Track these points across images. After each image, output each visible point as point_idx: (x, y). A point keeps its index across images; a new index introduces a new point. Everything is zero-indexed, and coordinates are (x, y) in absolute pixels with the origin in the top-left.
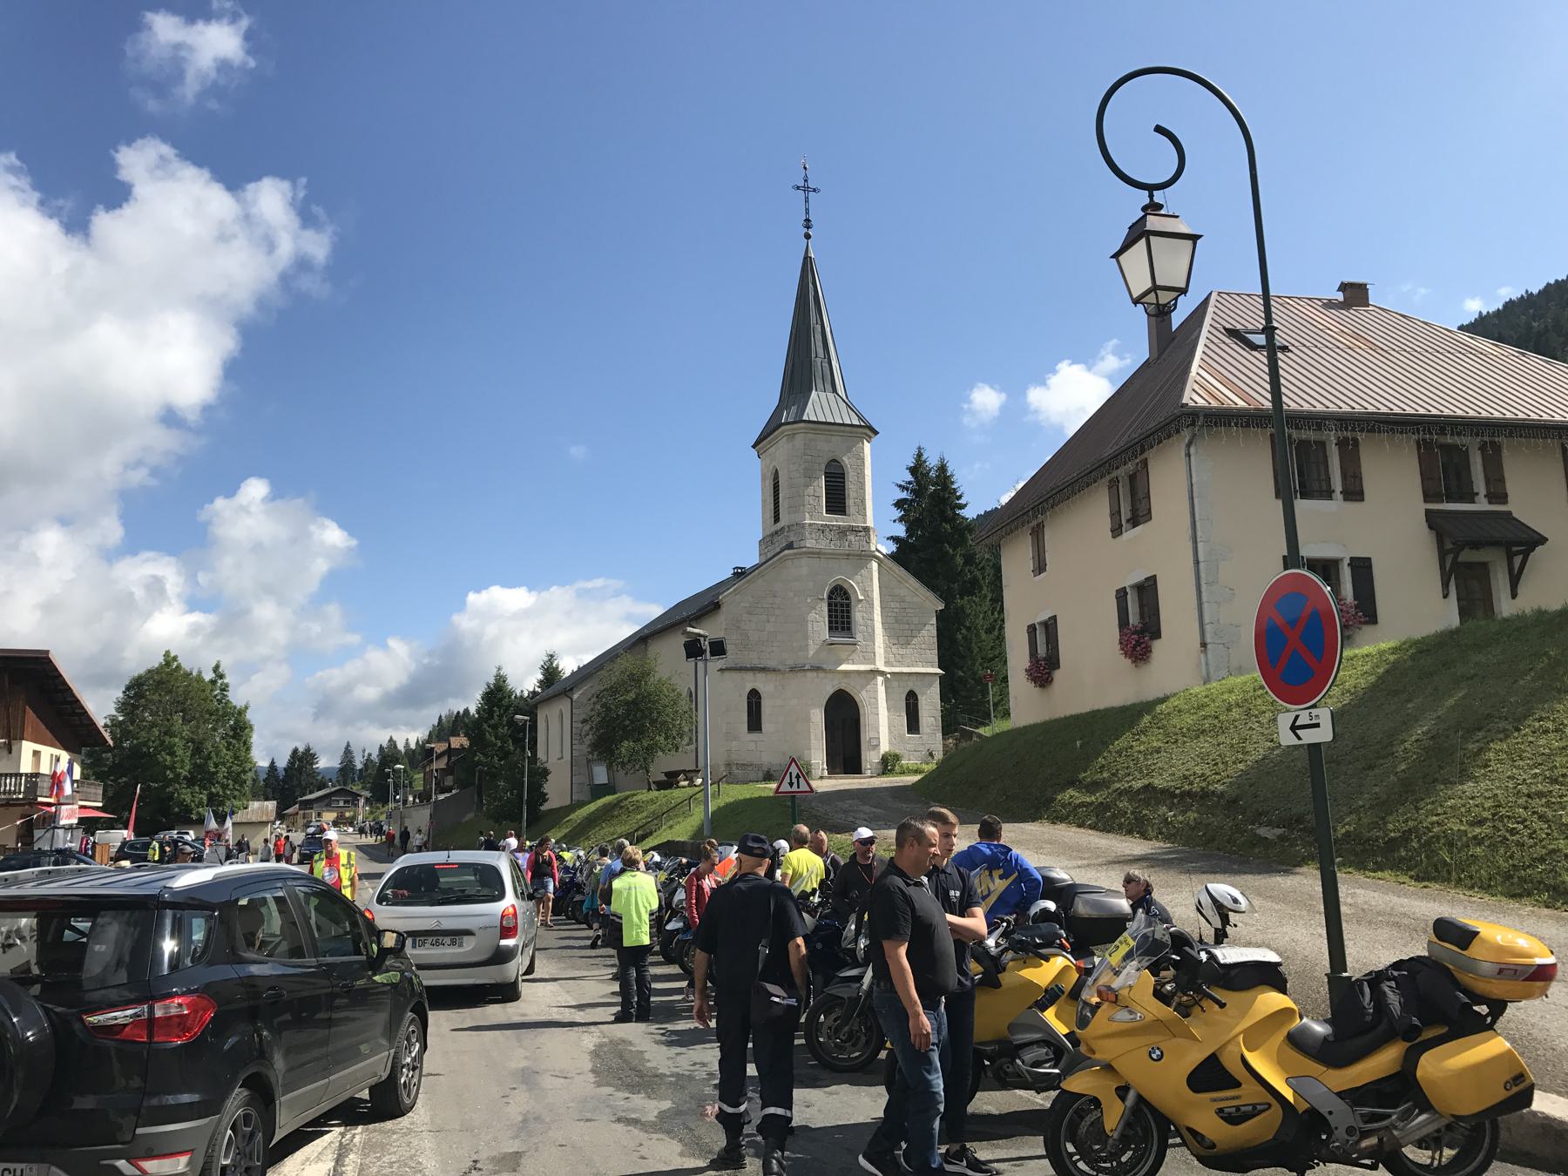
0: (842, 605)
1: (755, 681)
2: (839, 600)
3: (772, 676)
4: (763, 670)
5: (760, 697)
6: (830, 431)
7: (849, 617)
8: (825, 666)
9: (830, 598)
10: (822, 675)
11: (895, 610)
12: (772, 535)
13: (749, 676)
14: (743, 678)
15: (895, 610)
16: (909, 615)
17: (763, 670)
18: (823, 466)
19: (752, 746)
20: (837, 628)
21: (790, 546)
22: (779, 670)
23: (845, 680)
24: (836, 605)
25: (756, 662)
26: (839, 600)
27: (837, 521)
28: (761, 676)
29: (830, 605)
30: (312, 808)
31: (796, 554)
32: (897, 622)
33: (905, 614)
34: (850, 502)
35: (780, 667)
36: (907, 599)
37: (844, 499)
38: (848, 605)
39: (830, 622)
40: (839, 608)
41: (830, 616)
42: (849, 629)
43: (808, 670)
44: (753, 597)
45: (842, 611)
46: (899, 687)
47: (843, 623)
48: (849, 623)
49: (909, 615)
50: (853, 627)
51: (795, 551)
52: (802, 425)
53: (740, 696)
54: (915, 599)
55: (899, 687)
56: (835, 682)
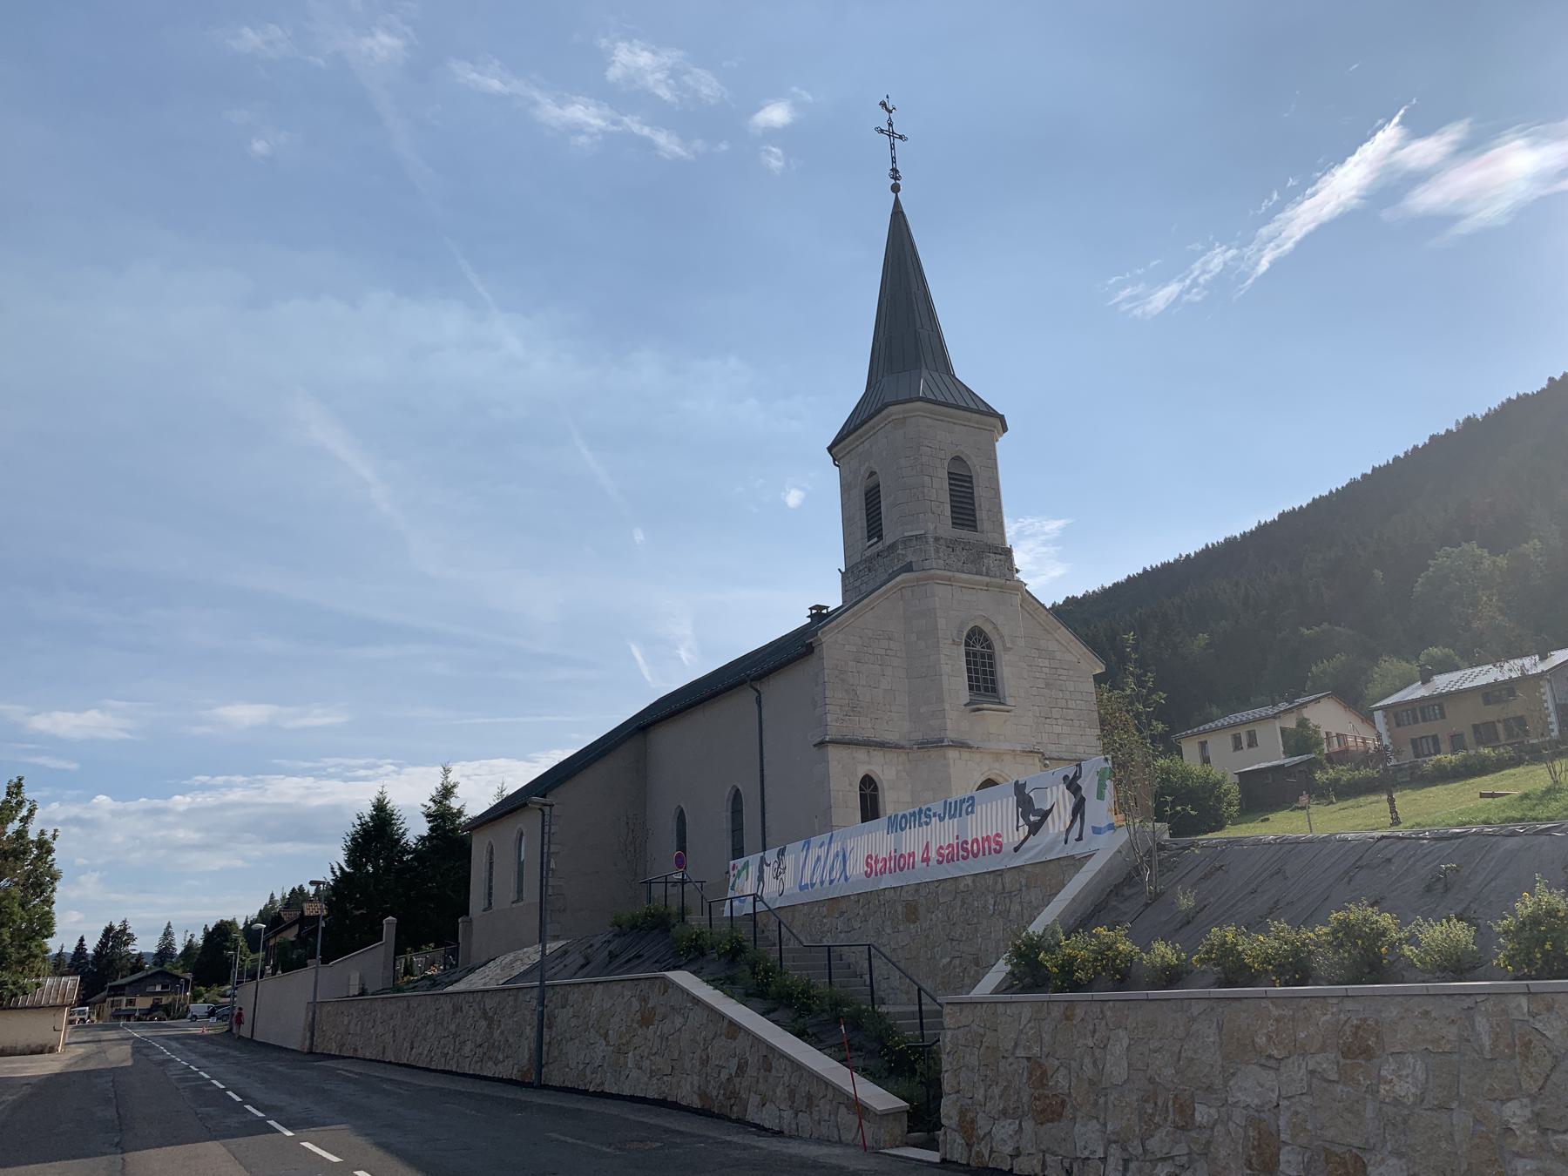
0: (983, 656)
2: (978, 648)
3: (892, 756)
4: (882, 745)
5: (876, 788)
6: (951, 417)
7: (992, 674)
10: (966, 754)
12: (870, 559)
13: (860, 754)
14: (853, 758)
16: (1061, 677)
17: (882, 745)
18: (946, 465)
20: (978, 688)
21: (908, 568)
22: (903, 747)
23: (997, 765)
24: (975, 655)
25: (868, 734)
26: (978, 648)
27: (964, 534)
28: (878, 755)
30: (123, 995)
31: (918, 580)
32: (1048, 685)
33: (1056, 677)
34: (982, 514)
35: (902, 743)
36: (1058, 655)
37: (974, 510)
38: (991, 657)
39: (970, 679)
40: (979, 660)
41: (969, 670)
42: (994, 690)
43: (949, 746)
44: (861, 637)
47: (985, 680)
48: (993, 682)
49: (1061, 677)
50: (1000, 687)
51: (917, 574)
52: (919, 404)
53: (851, 785)
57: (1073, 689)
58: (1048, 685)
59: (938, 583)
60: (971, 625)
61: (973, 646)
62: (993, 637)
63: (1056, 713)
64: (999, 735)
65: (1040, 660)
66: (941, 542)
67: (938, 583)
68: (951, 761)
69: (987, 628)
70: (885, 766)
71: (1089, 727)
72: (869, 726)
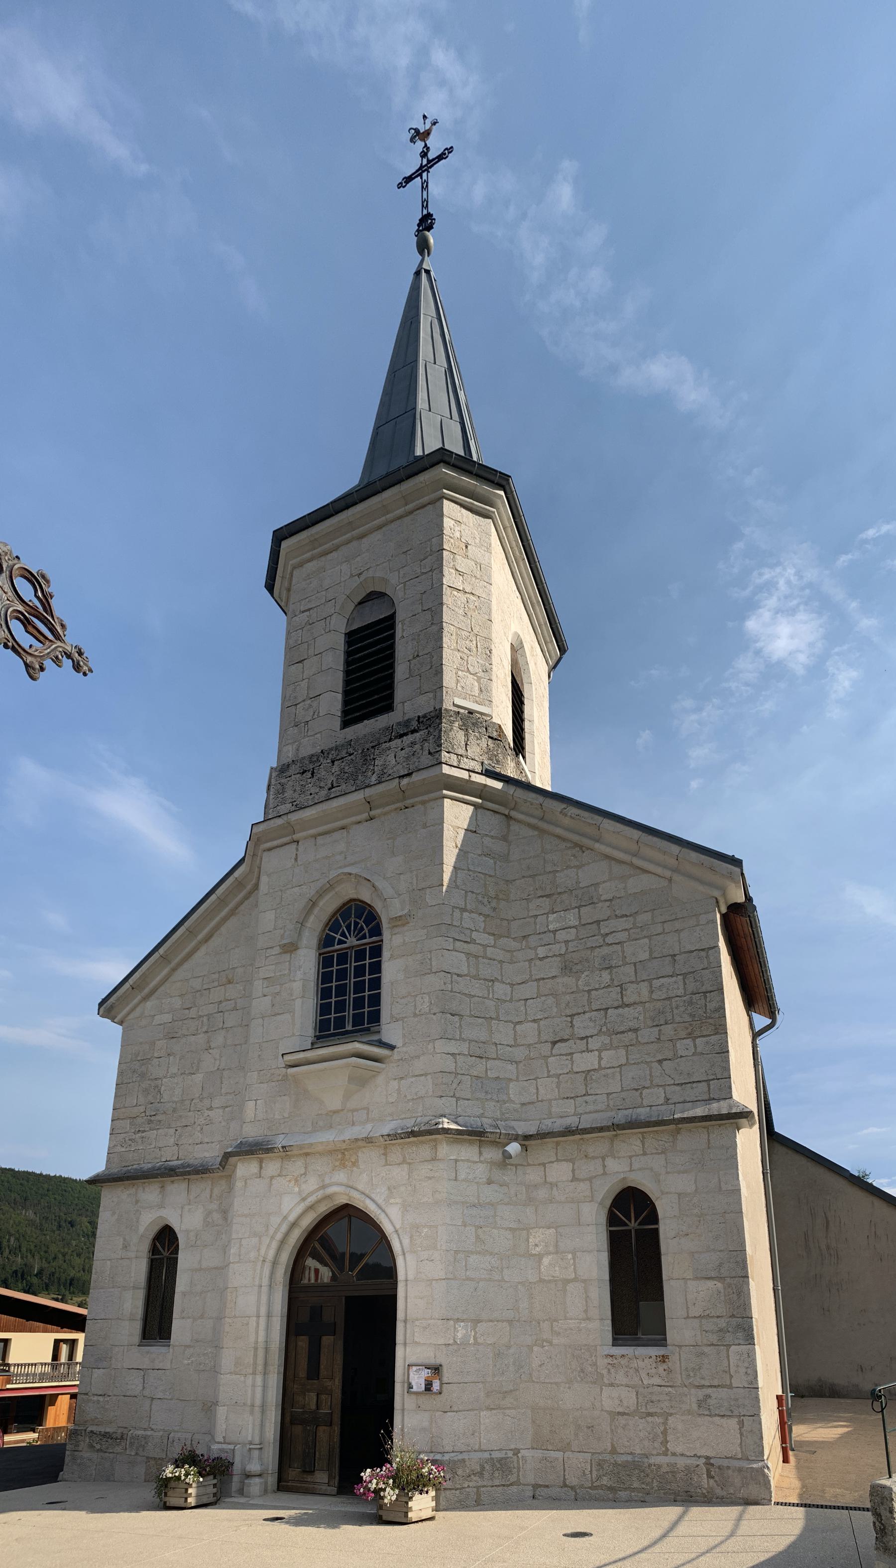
0: (360, 955)
1: (161, 1206)
2: (352, 941)
8: (280, 1141)
9: (326, 941)
10: (272, 1167)
11: (562, 936)
15: (562, 936)
16: (609, 940)
19: (134, 1384)
23: (341, 1176)
24: (343, 958)
26: (352, 941)
29: (325, 961)
32: (567, 969)
42: (375, 1017)
45: (360, 971)
46: (574, 1179)
49: (609, 940)
54: (637, 884)
55: (574, 1179)
56: (311, 1184)
57: (645, 956)
58: (567, 969)
59: (269, 850)
60: (329, 905)
61: (341, 942)
62: (378, 907)
63: (583, 1026)
64: (353, 1111)
65: (552, 917)
66: (294, 769)
67: (269, 850)
68: (239, 1184)
69: (366, 896)
70: (187, 1208)
71: (690, 1036)
72: (172, 1141)
